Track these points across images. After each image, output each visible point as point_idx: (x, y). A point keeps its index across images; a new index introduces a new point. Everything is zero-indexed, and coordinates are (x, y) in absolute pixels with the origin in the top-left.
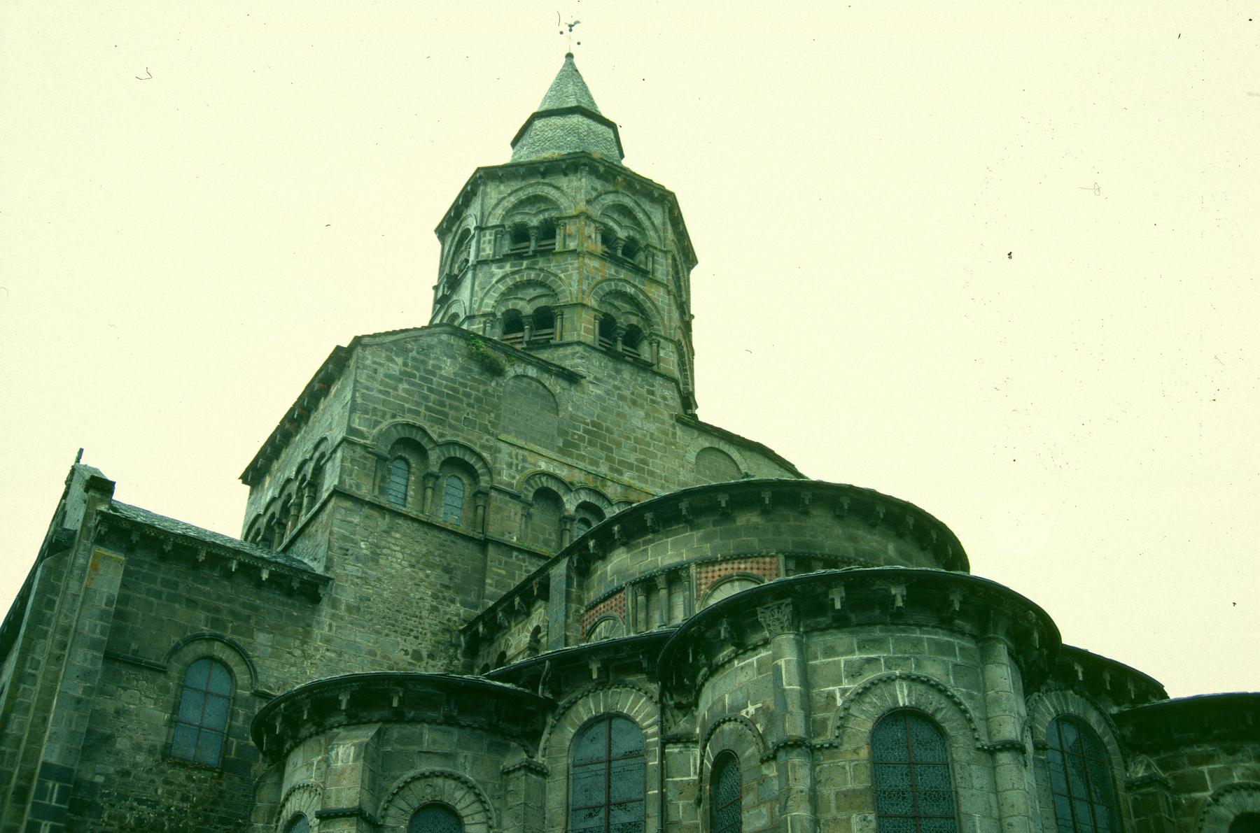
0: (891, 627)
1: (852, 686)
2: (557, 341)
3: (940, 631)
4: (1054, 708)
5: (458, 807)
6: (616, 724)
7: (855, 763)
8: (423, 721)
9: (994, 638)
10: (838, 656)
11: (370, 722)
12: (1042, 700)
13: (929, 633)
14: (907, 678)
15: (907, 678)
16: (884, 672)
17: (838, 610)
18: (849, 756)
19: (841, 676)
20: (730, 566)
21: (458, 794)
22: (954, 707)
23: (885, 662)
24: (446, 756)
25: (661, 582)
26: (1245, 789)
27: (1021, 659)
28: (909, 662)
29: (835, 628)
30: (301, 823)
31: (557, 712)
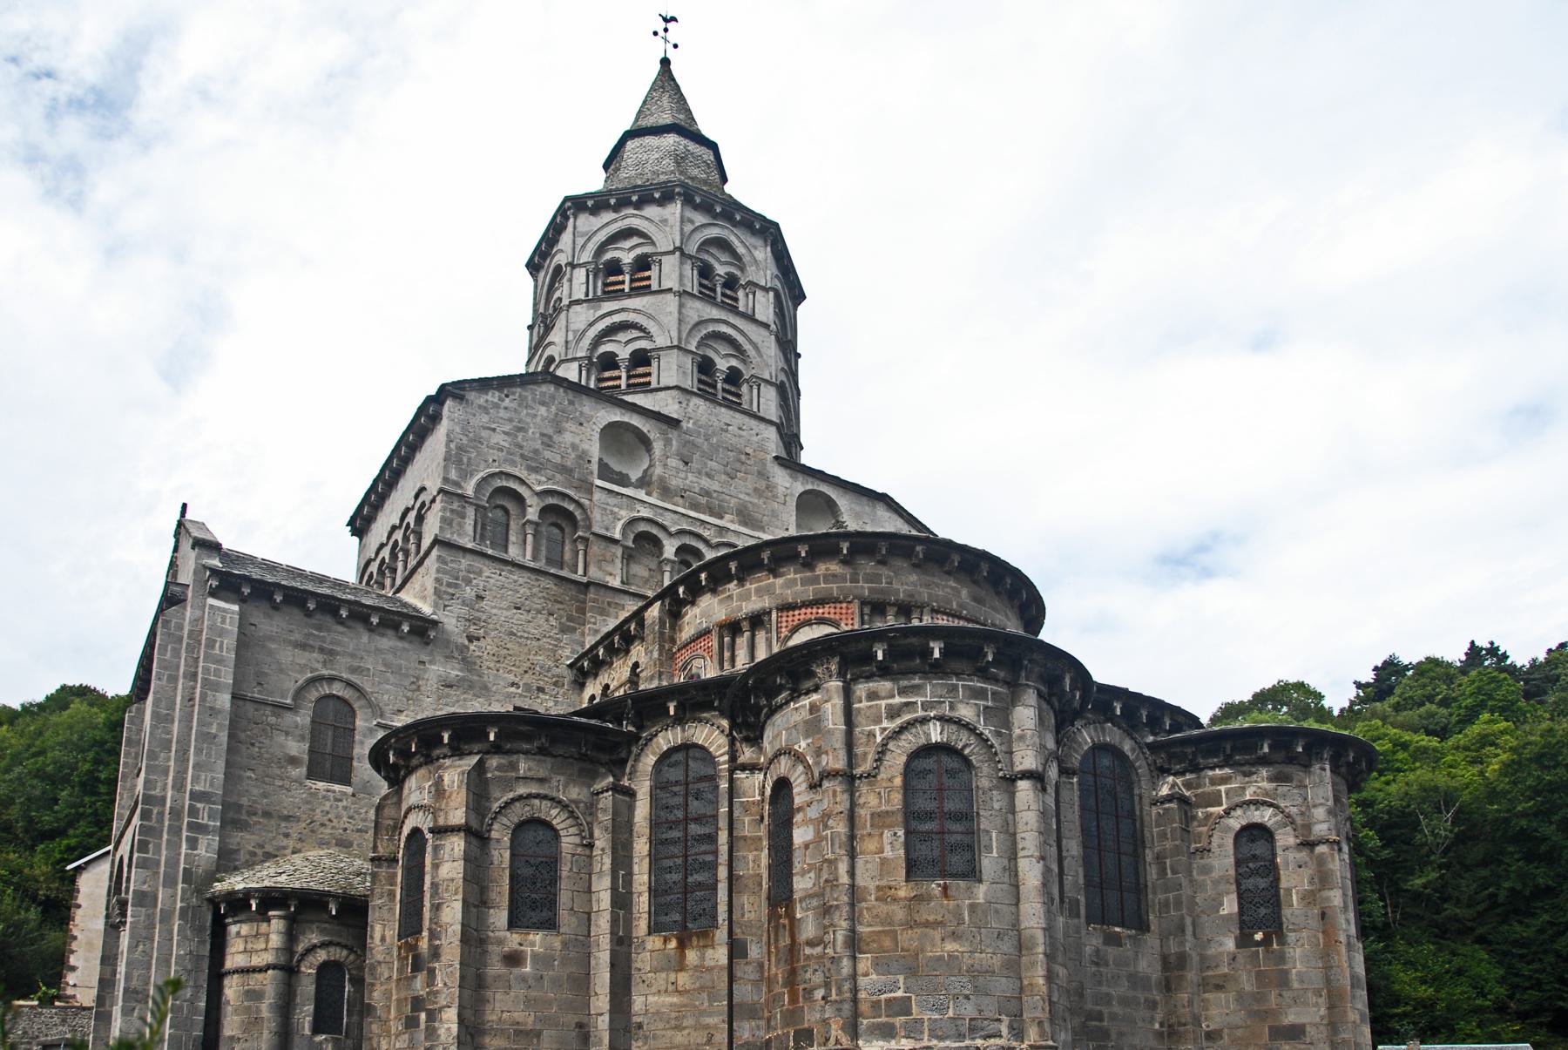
2: (654, 385)
3: (975, 678)
5: (554, 822)
6: (691, 752)
8: (518, 752)
11: (470, 753)
12: (1081, 732)
14: (941, 719)
15: (941, 719)
16: (920, 713)
18: (884, 785)
20: (809, 610)
21: (554, 812)
24: (542, 781)
25: (745, 625)
29: (879, 676)
30: (418, 835)
31: (640, 743)
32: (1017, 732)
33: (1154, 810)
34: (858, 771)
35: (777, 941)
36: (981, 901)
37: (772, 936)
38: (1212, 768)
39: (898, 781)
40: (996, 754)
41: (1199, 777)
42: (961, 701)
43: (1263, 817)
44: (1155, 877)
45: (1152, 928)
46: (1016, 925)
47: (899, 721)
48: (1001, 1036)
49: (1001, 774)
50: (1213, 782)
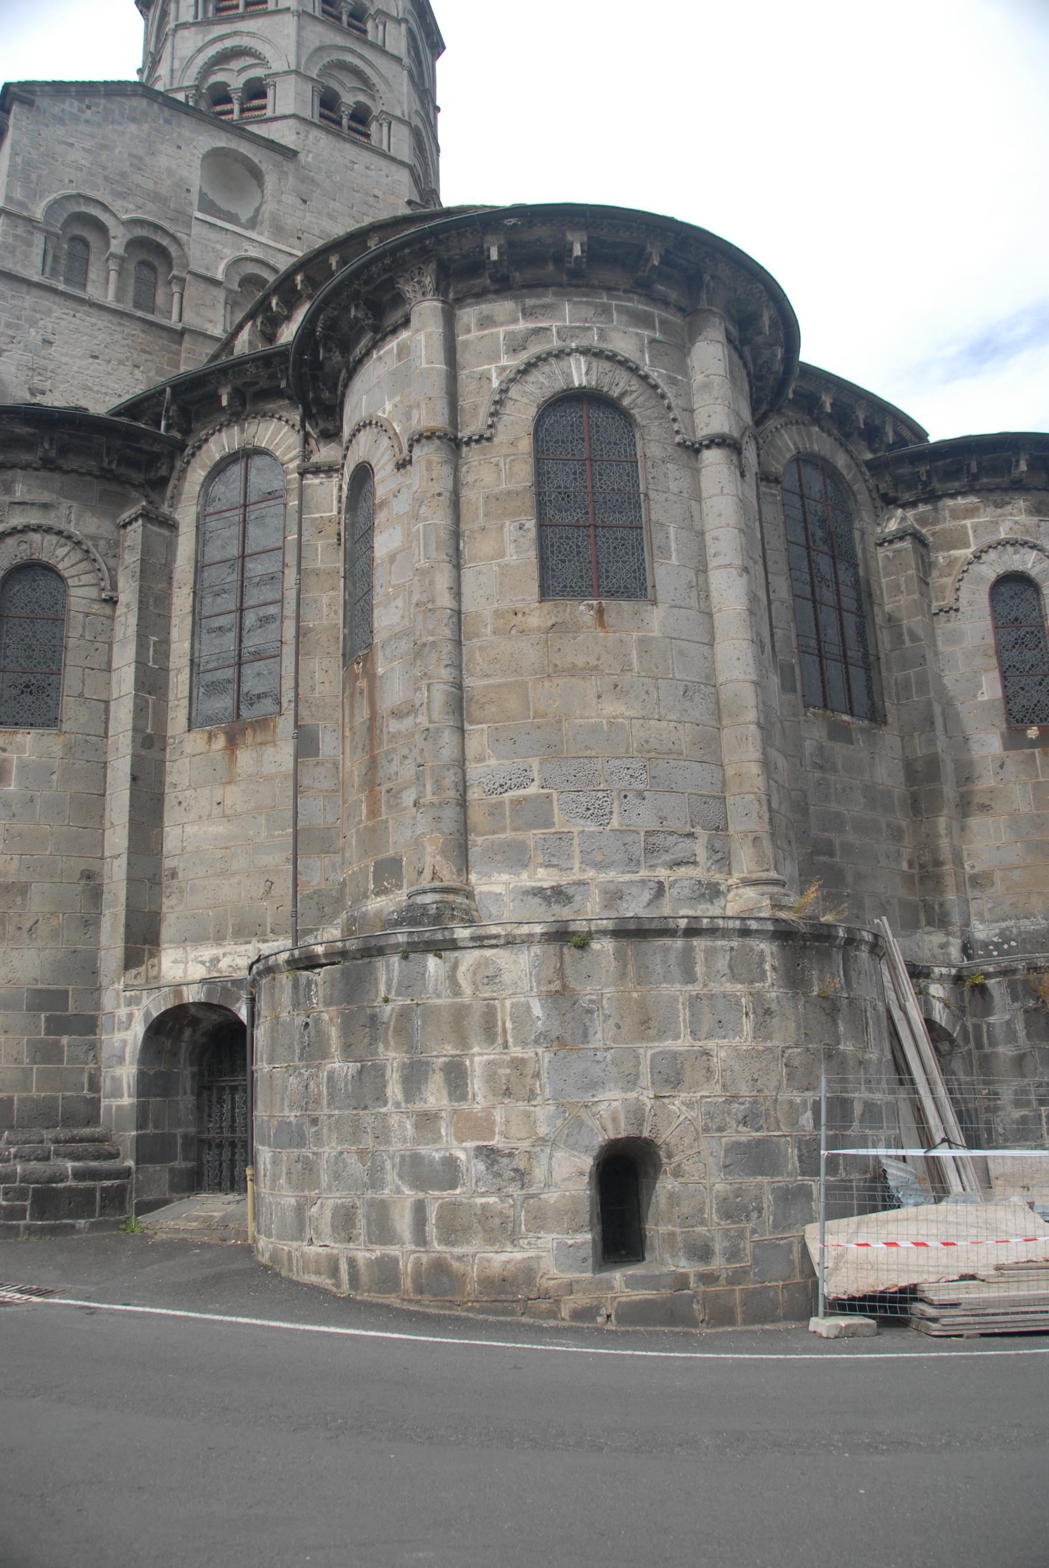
0: (569, 289)
1: (511, 362)
3: (635, 297)
4: (795, 444)
7: (513, 457)
9: (710, 311)
10: (496, 326)
12: (780, 434)
13: (619, 298)
15: (585, 352)
16: (556, 343)
17: (495, 262)
18: (504, 450)
19: (499, 351)
22: (650, 391)
23: (558, 332)
26: (1012, 545)
27: (746, 350)
28: (590, 333)
32: (698, 378)
33: (882, 553)
34: (463, 434)
35: (352, 716)
36: (656, 634)
37: (347, 713)
38: (953, 496)
39: (525, 445)
40: (669, 408)
41: (936, 510)
42: (616, 329)
43: (1025, 563)
44: (888, 647)
45: (890, 720)
46: (710, 679)
47: (524, 357)
48: (695, 863)
49: (678, 439)
50: (955, 516)
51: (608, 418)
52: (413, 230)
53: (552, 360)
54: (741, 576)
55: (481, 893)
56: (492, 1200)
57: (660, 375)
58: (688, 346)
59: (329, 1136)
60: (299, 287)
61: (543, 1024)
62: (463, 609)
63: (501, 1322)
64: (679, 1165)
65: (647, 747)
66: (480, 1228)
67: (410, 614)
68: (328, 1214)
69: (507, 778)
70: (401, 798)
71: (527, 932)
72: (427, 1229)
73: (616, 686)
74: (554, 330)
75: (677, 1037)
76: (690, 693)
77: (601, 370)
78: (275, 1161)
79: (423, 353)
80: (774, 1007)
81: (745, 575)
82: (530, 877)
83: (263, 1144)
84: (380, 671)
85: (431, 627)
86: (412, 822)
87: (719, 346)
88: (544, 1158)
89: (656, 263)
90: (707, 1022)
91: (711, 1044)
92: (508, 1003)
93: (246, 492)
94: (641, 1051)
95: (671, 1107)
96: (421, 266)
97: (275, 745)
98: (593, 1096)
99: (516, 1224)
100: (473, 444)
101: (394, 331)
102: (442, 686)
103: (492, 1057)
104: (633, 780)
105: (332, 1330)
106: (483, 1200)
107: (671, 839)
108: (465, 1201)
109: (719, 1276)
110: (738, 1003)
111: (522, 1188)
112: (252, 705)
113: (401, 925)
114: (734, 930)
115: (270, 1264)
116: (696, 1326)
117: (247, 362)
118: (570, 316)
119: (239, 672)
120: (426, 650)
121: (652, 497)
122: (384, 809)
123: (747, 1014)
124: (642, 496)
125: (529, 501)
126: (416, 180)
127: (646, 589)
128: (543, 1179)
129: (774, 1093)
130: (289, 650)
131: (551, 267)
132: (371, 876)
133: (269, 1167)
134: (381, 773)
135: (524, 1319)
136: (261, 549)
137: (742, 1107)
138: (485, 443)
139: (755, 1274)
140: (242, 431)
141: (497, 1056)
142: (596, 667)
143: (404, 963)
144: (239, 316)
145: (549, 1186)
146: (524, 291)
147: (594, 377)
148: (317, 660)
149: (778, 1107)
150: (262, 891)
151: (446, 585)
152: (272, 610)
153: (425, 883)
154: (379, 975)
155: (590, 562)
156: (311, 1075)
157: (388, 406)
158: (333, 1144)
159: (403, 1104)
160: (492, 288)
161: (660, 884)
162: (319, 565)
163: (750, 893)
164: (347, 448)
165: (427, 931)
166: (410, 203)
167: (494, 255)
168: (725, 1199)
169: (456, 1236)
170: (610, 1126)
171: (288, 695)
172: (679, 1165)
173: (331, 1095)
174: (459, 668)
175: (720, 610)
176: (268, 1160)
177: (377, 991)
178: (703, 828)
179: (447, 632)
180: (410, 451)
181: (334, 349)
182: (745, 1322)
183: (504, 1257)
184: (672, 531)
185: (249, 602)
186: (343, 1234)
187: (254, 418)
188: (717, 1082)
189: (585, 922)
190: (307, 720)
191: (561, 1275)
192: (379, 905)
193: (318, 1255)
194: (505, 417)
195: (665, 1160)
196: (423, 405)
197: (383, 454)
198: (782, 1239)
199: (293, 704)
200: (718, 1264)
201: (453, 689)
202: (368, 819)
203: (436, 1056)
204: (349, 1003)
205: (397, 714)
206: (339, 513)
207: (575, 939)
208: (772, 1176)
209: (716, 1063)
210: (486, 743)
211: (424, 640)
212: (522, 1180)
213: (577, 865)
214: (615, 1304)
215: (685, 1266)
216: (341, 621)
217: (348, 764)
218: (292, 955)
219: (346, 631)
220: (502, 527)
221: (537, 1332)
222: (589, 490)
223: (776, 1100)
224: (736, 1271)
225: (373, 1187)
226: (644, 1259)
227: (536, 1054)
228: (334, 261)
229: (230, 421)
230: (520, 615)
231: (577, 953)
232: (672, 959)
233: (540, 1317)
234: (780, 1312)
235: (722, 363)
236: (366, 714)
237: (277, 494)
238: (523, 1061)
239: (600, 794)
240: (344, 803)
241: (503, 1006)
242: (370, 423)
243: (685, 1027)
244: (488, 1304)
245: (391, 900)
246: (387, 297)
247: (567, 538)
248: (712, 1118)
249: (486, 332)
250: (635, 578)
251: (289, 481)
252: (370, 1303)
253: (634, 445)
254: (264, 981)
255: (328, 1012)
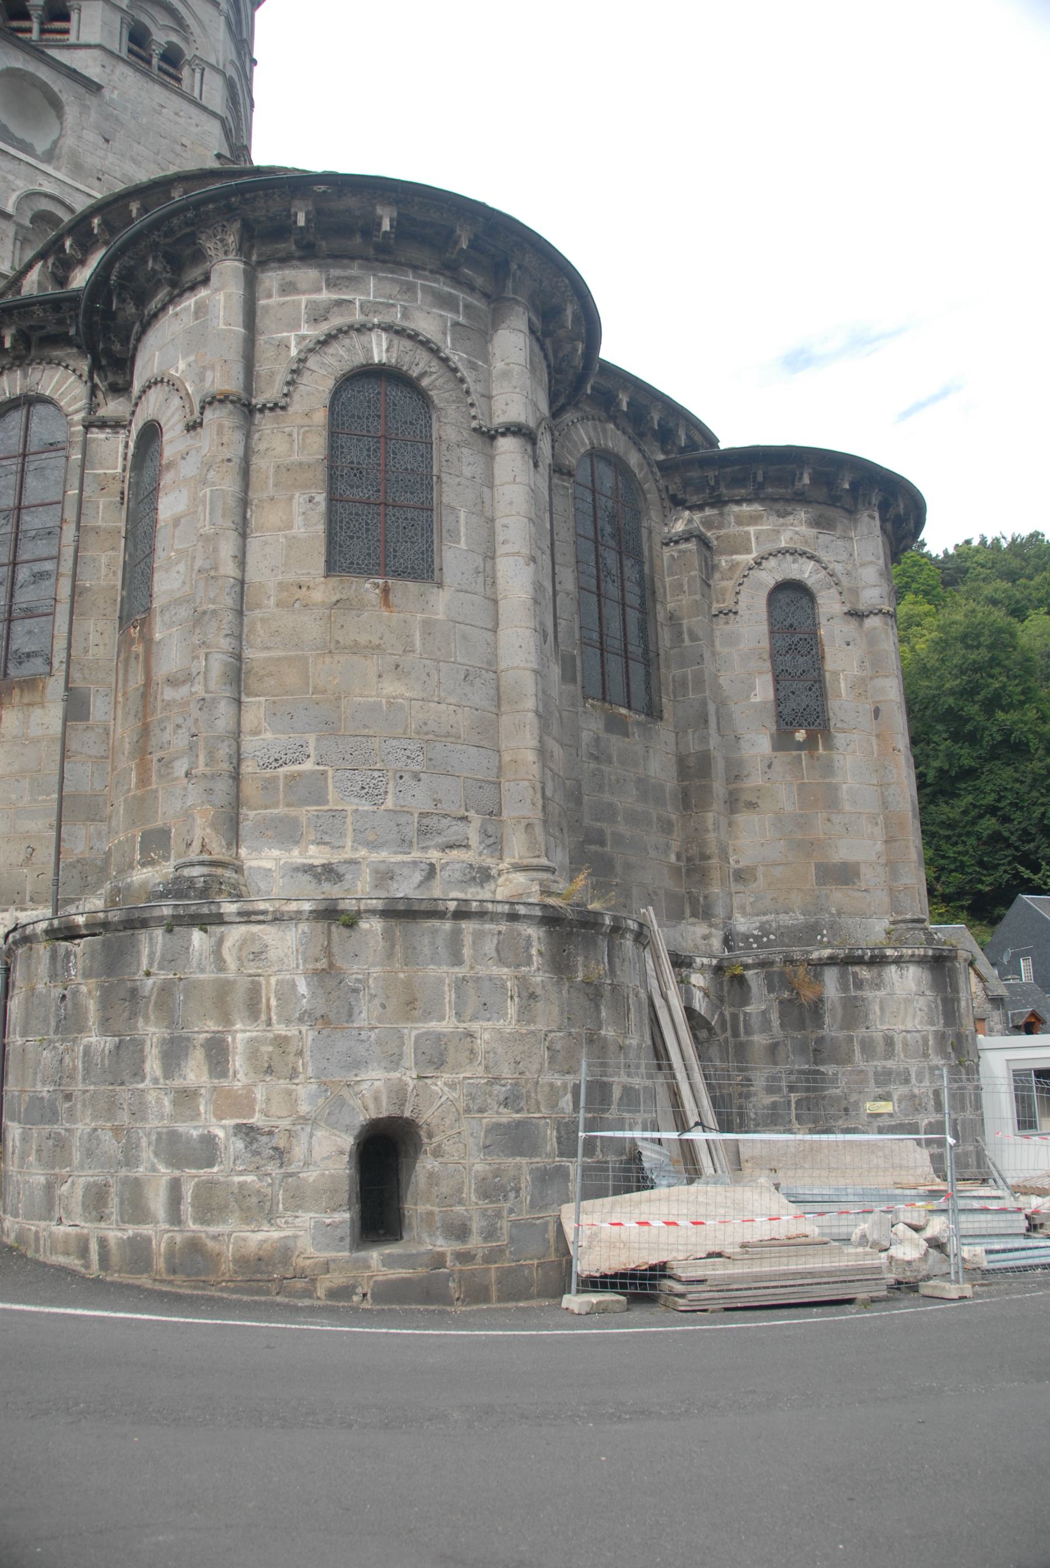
1: (311, 332)
3: (442, 279)
4: (589, 439)
9: (514, 299)
10: (298, 294)
12: (576, 428)
13: (424, 278)
14: (387, 328)
15: (387, 328)
16: (358, 317)
17: (301, 228)
18: (299, 421)
19: (299, 319)
22: (449, 374)
23: (361, 306)
26: (792, 554)
27: (548, 342)
28: (393, 310)
32: (499, 366)
33: (667, 552)
34: (258, 401)
35: (126, 680)
38: (738, 502)
39: (321, 417)
40: (468, 392)
41: (721, 514)
42: (419, 308)
43: (802, 572)
44: (668, 644)
45: (666, 715)
46: (492, 664)
47: (324, 328)
48: (467, 847)
49: (474, 424)
50: (739, 522)
51: (405, 397)
52: (218, 185)
53: (354, 334)
54: (528, 565)
55: (250, 868)
56: (250, 1178)
57: (461, 359)
58: (490, 332)
59: (83, 1112)
60: (96, 231)
61: (308, 1002)
62: (247, 579)
63: (255, 1302)
64: (439, 1146)
65: (425, 729)
66: (236, 1207)
67: (191, 580)
68: (79, 1192)
69: (283, 752)
70: (173, 768)
71: (295, 909)
72: (182, 1207)
73: (397, 666)
74: (358, 303)
75: (442, 1018)
76: (471, 678)
77: (401, 348)
78: (25, 1138)
79: (222, 313)
80: (539, 991)
81: (532, 564)
82: (301, 854)
83: (12, 1120)
84: (158, 636)
85: (212, 595)
86: (183, 793)
87: (521, 335)
88: (304, 1137)
89: (465, 247)
90: (472, 1004)
91: (475, 1026)
92: (273, 980)
93: (25, 442)
94: (406, 1031)
95: (433, 1087)
96: (225, 223)
97: (43, 707)
98: (356, 1075)
99: (274, 1202)
100: (267, 411)
101: (193, 288)
102: (220, 656)
103: (255, 1034)
104: (409, 761)
105: (79, 1312)
106: (241, 1179)
107: (445, 822)
108: (222, 1179)
109: (476, 1255)
110: (504, 986)
111: (281, 1166)
112: (20, 663)
113: (166, 897)
114: (503, 914)
115: (16, 1245)
116: (451, 1304)
117: (33, 304)
118: (374, 291)
119: (9, 628)
120: (207, 618)
121: (444, 480)
122: (154, 778)
123: (512, 997)
124: (435, 478)
125: (321, 474)
126: (227, 133)
127: (433, 572)
128: (302, 1157)
129: (536, 1076)
130: (62, 610)
131: (358, 240)
132: (138, 846)
133: (18, 1144)
134: (153, 741)
135: (279, 1299)
136: (39, 502)
137: (504, 1089)
138: (279, 412)
139: (511, 1252)
140: (25, 376)
141: (260, 1034)
142: (378, 646)
143: (168, 936)
144: (29, 254)
145: (309, 1165)
146: (329, 261)
147: (395, 355)
148: (92, 622)
149: (539, 1089)
150: (22, 857)
151: (230, 553)
152: (48, 566)
153: (193, 855)
154: (142, 947)
155: (378, 541)
156: (67, 1050)
157: (182, 365)
158: (87, 1121)
159: (162, 1081)
160: (297, 254)
161: (432, 866)
162: (100, 523)
163: (520, 878)
164: (136, 405)
165: (193, 905)
166: (219, 156)
167: (301, 221)
168: (484, 1179)
169: (212, 1215)
170: (371, 1106)
171: (59, 657)
172: (439, 1146)
173: (87, 1070)
174: (239, 638)
175: (505, 597)
176: (17, 1137)
177: (139, 964)
178: (477, 812)
179: (229, 601)
180: (202, 414)
181: (129, 300)
182: (500, 1300)
183: (260, 1236)
184: (462, 515)
185: (23, 556)
186: (94, 1213)
187: (39, 364)
188: (480, 1064)
189: (354, 901)
190: (78, 682)
191: (317, 1254)
192: (143, 876)
193: (67, 1235)
194: (302, 387)
195: (425, 1140)
196: (218, 368)
197: (173, 415)
198: (538, 1218)
199: (64, 666)
200: (475, 1243)
201: (232, 660)
202: (137, 787)
203: (198, 1032)
204: (109, 976)
205: (172, 682)
206: (124, 470)
207: (344, 918)
208: (531, 1156)
209: (480, 1045)
210: (262, 716)
211: (204, 607)
212: (281, 1158)
213: (349, 844)
214: (372, 1283)
215: (443, 1245)
216: (119, 583)
217: (119, 730)
218: (51, 925)
219: (124, 593)
220: (291, 498)
221: (292, 1312)
222: (382, 468)
223: (537, 1083)
224: (492, 1250)
225: (127, 1165)
226: (401, 1238)
227: (300, 1032)
228: (134, 207)
229: (13, 365)
230: (304, 589)
231: (345, 932)
232: (440, 942)
233: (295, 1297)
234: (534, 1290)
235: (522, 353)
236: (141, 679)
237: (59, 446)
238: (286, 1039)
239: (376, 774)
240: (113, 770)
241: (268, 983)
242: (162, 381)
243: (450, 1008)
244: (243, 1284)
245: (157, 872)
246: (188, 252)
247: (357, 514)
248: (473, 1099)
249: (288, 298)
250: (423, 559)
251: (73, 434)
252: (121, 1283)
253: (430, 427)
254: (20, 951)
255: (86, 985)
